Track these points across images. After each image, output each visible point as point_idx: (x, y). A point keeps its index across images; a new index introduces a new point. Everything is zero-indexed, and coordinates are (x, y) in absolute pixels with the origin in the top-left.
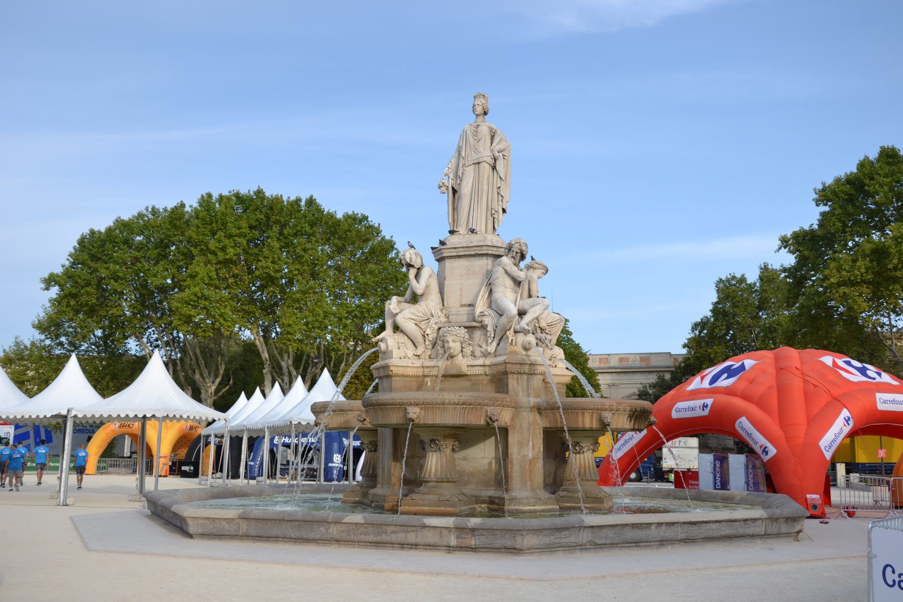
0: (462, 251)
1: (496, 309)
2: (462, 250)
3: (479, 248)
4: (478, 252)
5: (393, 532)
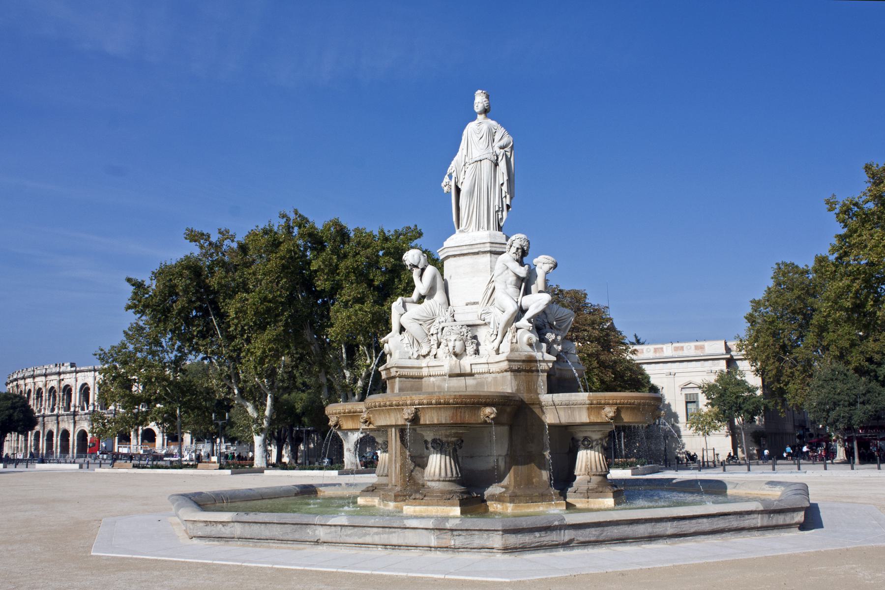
0: (466, 249)
1: (498, 306)
2: (465, 248)
3: (482, 245)
4: (482, 250)
5: (377, 534)
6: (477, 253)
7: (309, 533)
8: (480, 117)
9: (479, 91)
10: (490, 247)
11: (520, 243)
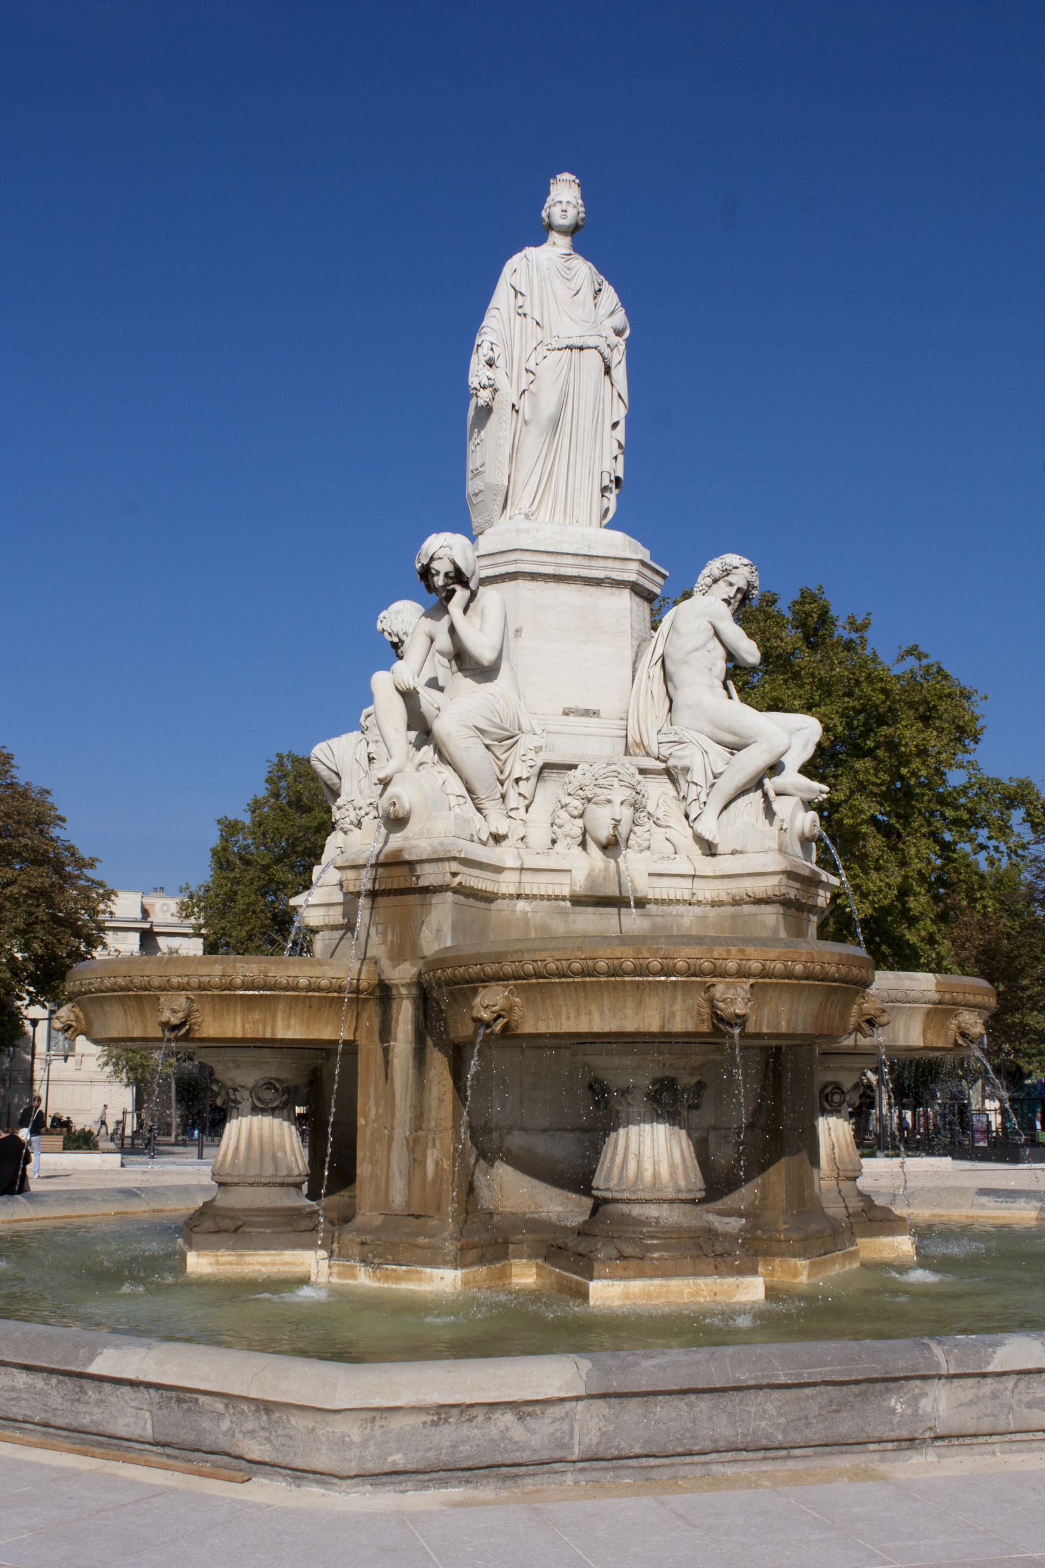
0: (572, 566)
2: (570, 560)
3: (618, 565)
4: (615, 575)
6: (598, 582)
7: (893, 1411)
8: (558, 245)
9: (567, 176)
10: (639, 573)
11: (749, 577)
